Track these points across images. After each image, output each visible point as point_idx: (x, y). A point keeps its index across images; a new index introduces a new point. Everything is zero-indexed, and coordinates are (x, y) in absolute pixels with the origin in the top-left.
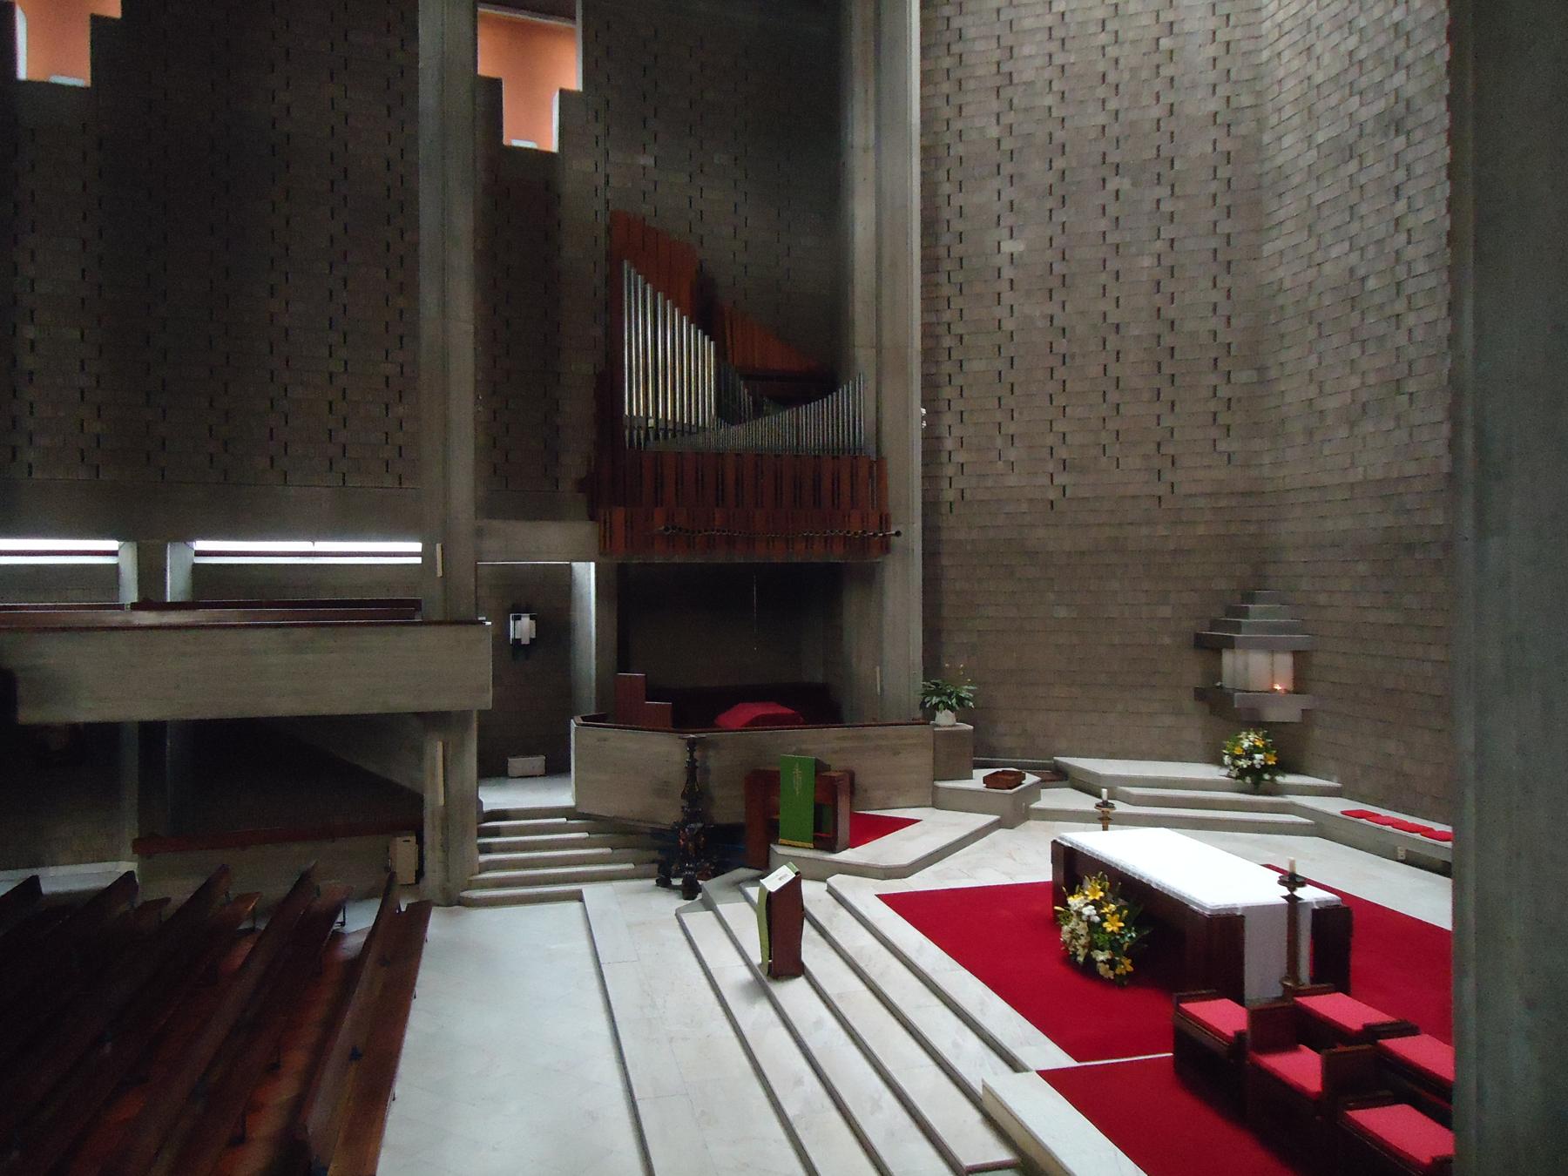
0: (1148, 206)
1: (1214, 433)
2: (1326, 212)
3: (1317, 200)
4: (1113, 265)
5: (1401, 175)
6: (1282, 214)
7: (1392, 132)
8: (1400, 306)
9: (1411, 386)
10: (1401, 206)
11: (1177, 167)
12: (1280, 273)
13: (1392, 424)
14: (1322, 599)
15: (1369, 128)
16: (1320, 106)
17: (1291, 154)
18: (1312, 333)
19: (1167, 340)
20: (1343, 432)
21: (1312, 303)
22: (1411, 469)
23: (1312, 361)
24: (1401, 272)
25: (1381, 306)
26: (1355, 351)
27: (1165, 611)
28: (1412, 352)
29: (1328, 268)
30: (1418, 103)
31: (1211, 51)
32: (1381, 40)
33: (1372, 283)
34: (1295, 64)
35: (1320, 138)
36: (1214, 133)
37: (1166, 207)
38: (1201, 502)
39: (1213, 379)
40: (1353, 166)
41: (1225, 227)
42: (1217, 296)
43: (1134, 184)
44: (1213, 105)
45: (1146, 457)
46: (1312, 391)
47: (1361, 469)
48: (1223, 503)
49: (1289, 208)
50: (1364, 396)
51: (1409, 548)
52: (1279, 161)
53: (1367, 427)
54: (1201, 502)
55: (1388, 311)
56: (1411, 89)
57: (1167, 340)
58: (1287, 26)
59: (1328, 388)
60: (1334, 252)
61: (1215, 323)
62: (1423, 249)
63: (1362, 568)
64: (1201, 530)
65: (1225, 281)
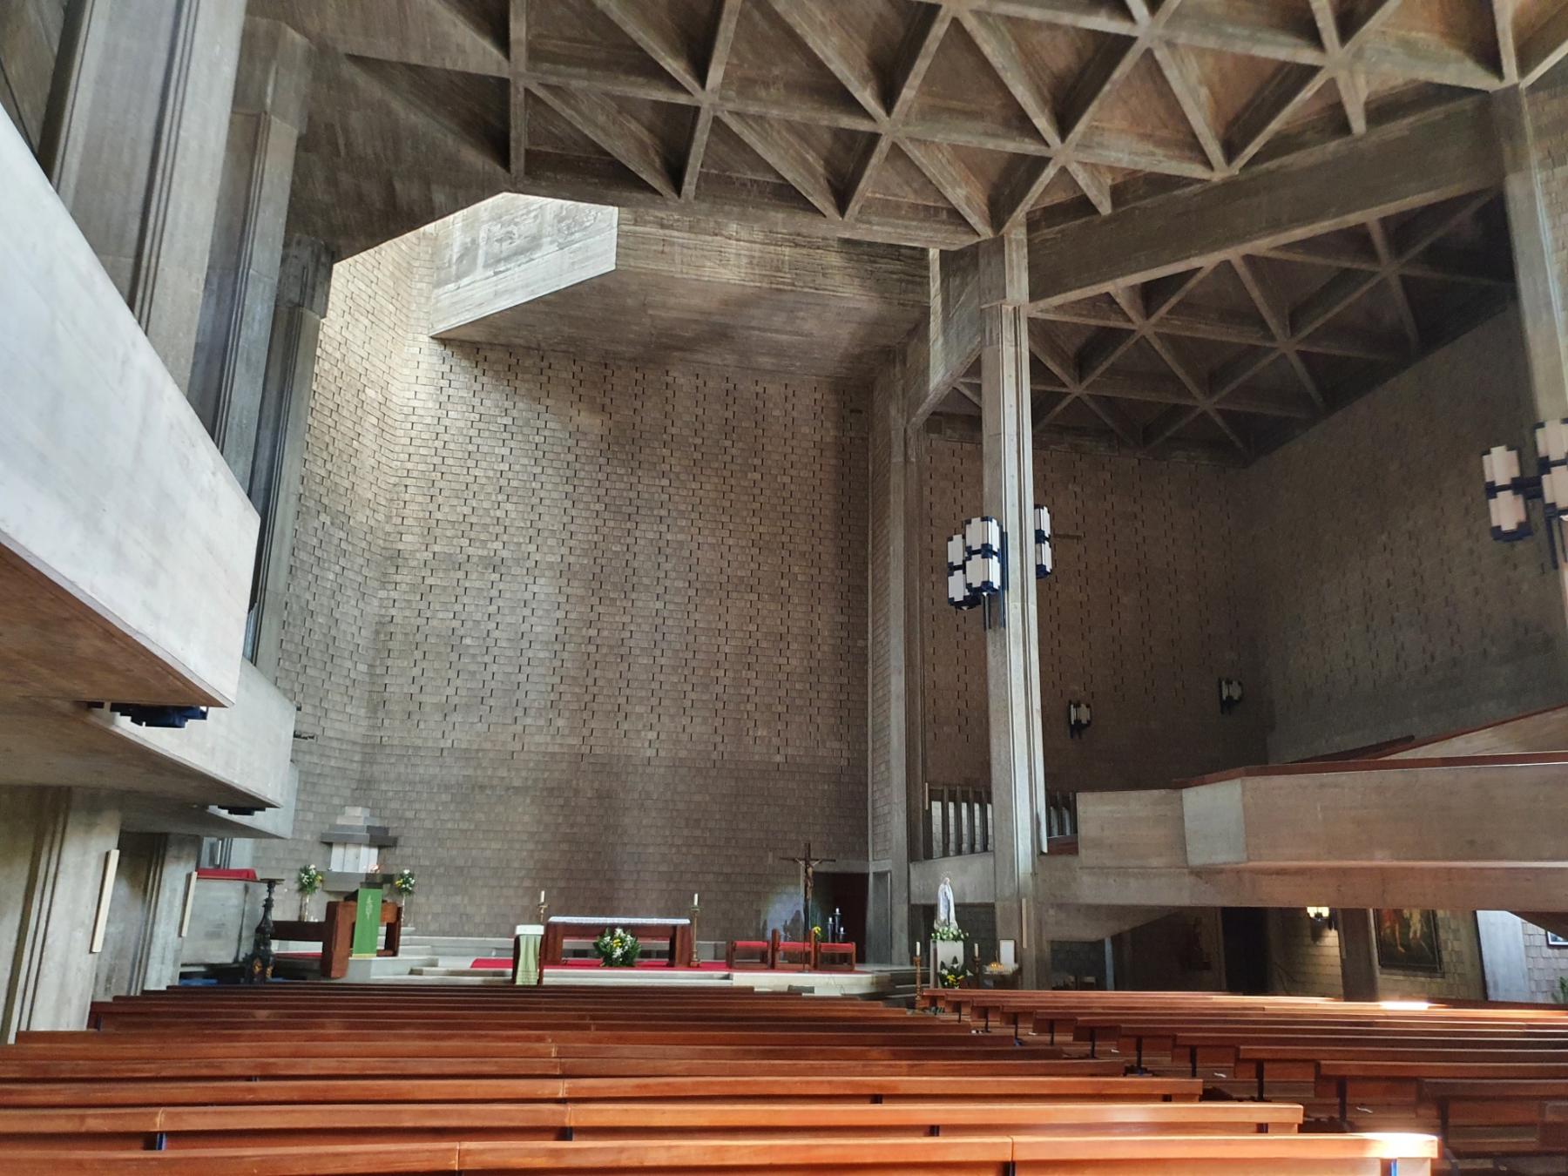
0: (336, 542)
1: (346, 699)
2: (436, 591)
3: (429, 581)
4: (316, 570)
5: (494, 593)
6: (398, 578)
7: (491, 570)
8: (487, 659)
9: (492, 702)
10: (493, 609)
11: (351, 523)
12: (393, 612)
13: (476, 720)
14: (410, 814)
15: (474, 560)
16: (438, 532)
17: (409, 548)
18: (418, 655)
19: (333, 632)
20: (438, 717)
21: (419, 637)
22: (488, 745)
23: (416, 672)
24: (490, 641)
25: (474, 656)
26: (452, 674)
27: (310, 816)
28: (493, 684)
29: (434, 623)
30: (510, 563)
31: (372, 462)
32: (488, 520)
33: (468, 641)
34: (420, 499)
35: (437, 548)
36: (368, 512)
37: (344, 545)
38: (335, 744)
39: (349, 664)
40: (461, 574)
41: (365, 571)
42: (357, 613)
43: (332, 524)
44: (370, 496)
45: (315, 707)
46: (415, 689)
47: (450, 741)
48: (344, 747)
49: (404, 577)
50: (456, 700)
51: (482, 788)
52: (400, 546)
53: (456, 718)
54: (335, 744)
55: (479, 659)
56: (505, 554)
57: (333, 632)
58: (415, 474)
59: (427, 689)
60: (440, 615)
61: (354, 629)
62: (505, 635)
63: (445, 797)
64: (333, 763)
65: (361, 605)
